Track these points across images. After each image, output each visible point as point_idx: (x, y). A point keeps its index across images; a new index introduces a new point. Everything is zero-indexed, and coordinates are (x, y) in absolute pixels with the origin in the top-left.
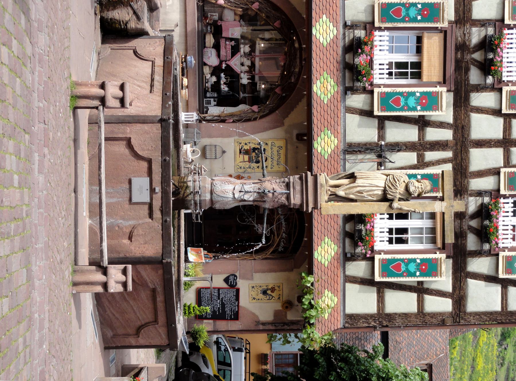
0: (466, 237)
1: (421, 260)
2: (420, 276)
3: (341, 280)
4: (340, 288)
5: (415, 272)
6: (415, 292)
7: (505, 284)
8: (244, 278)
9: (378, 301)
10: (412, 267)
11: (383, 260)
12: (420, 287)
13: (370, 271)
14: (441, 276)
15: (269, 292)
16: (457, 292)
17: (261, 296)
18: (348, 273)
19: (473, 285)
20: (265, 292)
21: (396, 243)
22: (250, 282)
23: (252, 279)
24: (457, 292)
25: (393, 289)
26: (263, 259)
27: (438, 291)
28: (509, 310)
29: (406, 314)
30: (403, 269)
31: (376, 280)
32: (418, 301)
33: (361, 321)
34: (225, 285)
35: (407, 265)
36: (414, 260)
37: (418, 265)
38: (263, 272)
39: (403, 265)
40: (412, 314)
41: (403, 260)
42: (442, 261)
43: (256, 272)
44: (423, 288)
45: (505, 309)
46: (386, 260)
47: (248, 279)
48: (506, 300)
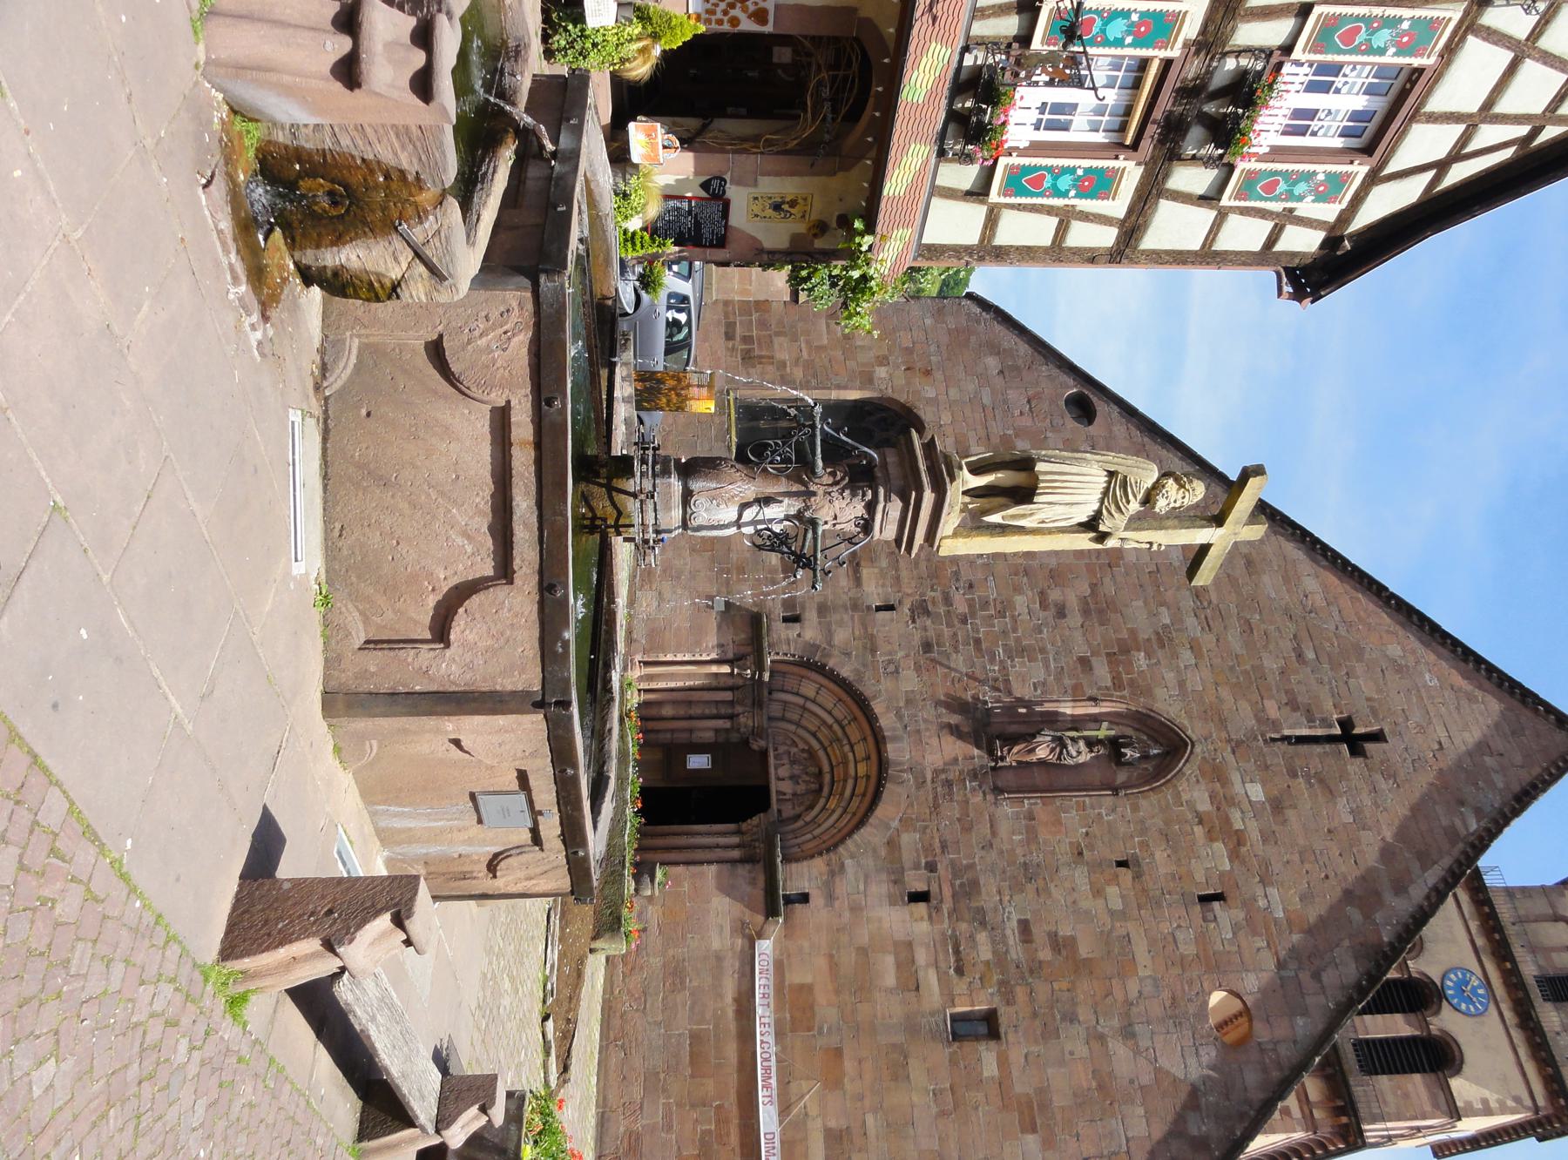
0: (1186, 131)
1: (1085, 170)
2: (1076, 196)
4: (921, 206)
5: (1068, 191)
8: (738, 182)
9: (985, 227)
10: (1065, 182)
11: (1013, 167)
15: (785, 207)
16: (1133, 218)
17: (770, 212)
19: (1166, 210)
20: (777, 207)
21: (1046, 129)
22: (752, 190)
23: (755, 184)
24: (1133, 218)
26: (778, 153)
29: (1029, 248)
30: (1048, 183)
34: (703, 194)
35: (1056, 178)
36: (1072, 170)
37: (1081, 179)
38: (777, 174)
39: (1048, 177)
41: (1050, 169)
43: (763, 174)
46: (1018, 167)
47: (746, 185)
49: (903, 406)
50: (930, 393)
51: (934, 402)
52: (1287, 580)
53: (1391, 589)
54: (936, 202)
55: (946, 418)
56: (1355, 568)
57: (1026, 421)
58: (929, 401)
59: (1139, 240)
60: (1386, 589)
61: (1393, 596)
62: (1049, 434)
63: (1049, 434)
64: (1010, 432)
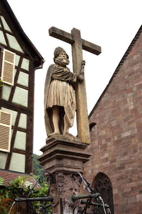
3: (6, 172)
6: (16, 131)
7: (16, 84)
12: (14, 128)
13: (4, 154)
14: (10, 115)
16: (18, 109)
18: (4, 168)
19: (15, 100)
24: (18, 109)
25: (14, 143)
27: (16, 119)
28: (28, 86)
31: (9, 152)
32: (21, 131)
33: (29, 165)
40: (27, 136)
42: (2, 112)
44: (15, 126)
45: (27, 88)
48: (23, 86)
49: (94, 180)
50: (90, 171)
51: (92, 170)
52: (135, 64)
53: (134, 38)
54: (11, 168)
55: (97, 166)
56: (129, 48)
57: (96, 142)
58: (92, 172)
59: (24, 107)
60: (134, 39)
61: (135, 37)
62: (100, 135)
63: (100, 135)
64: (100, 146)
